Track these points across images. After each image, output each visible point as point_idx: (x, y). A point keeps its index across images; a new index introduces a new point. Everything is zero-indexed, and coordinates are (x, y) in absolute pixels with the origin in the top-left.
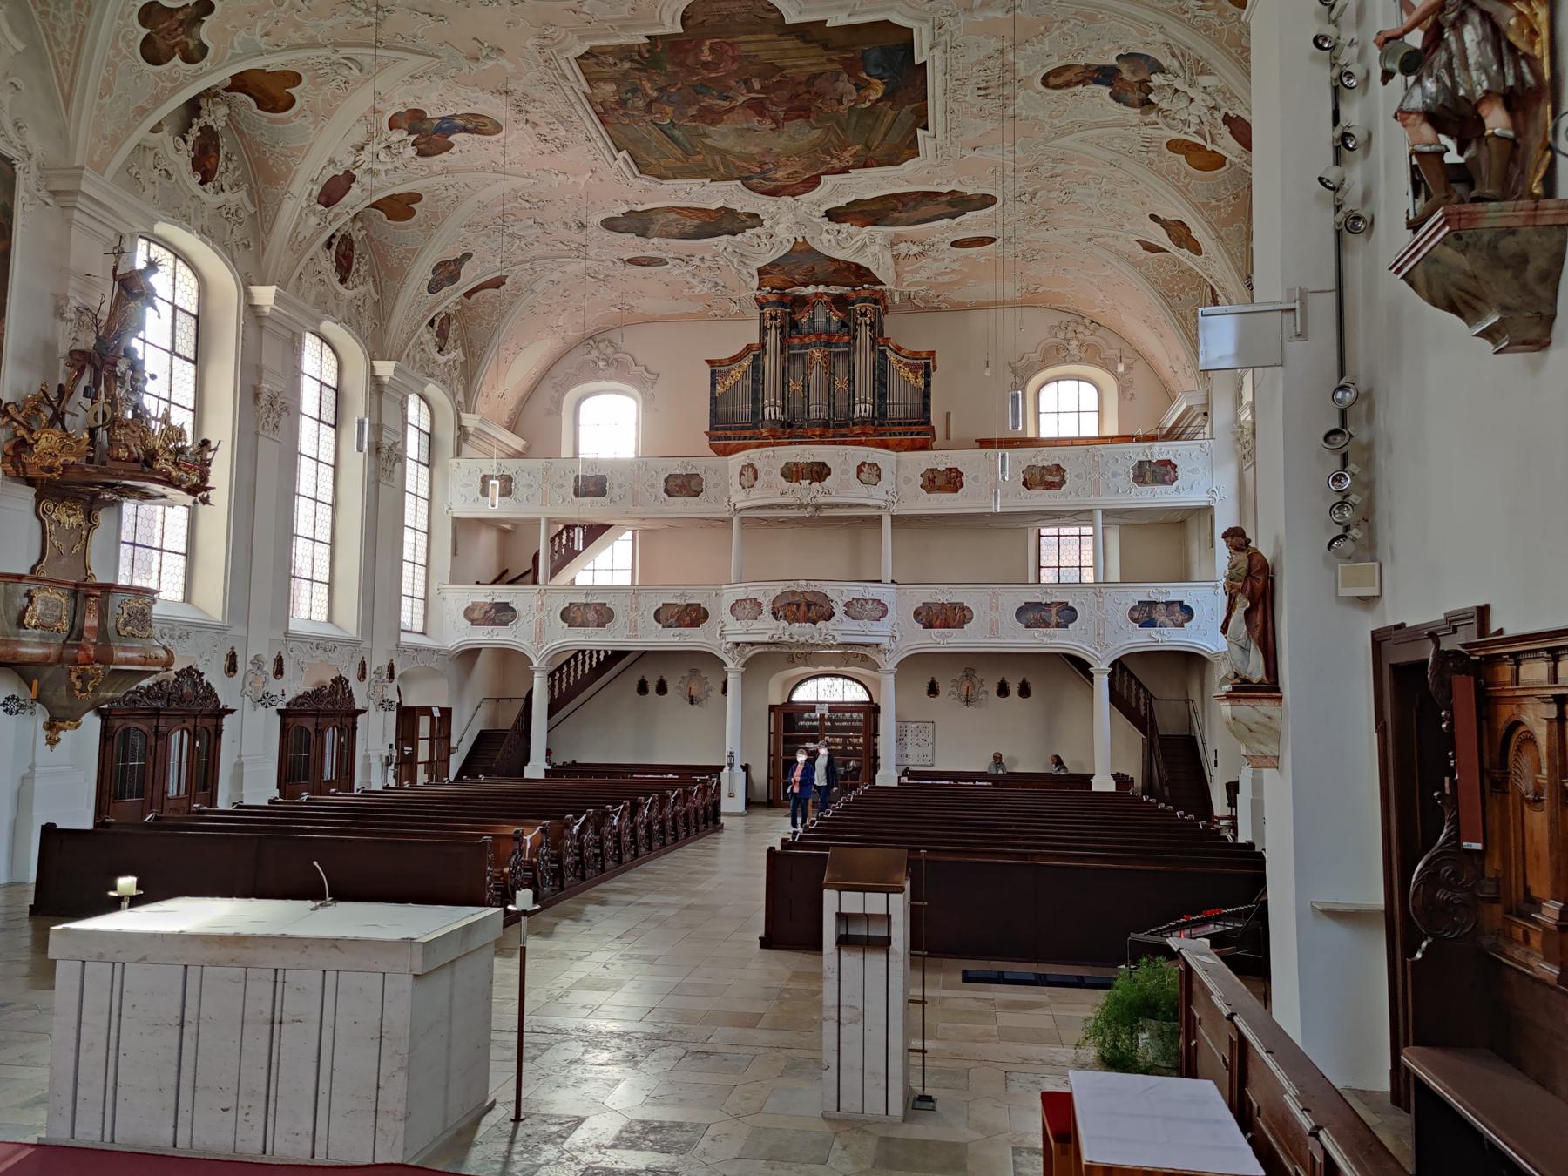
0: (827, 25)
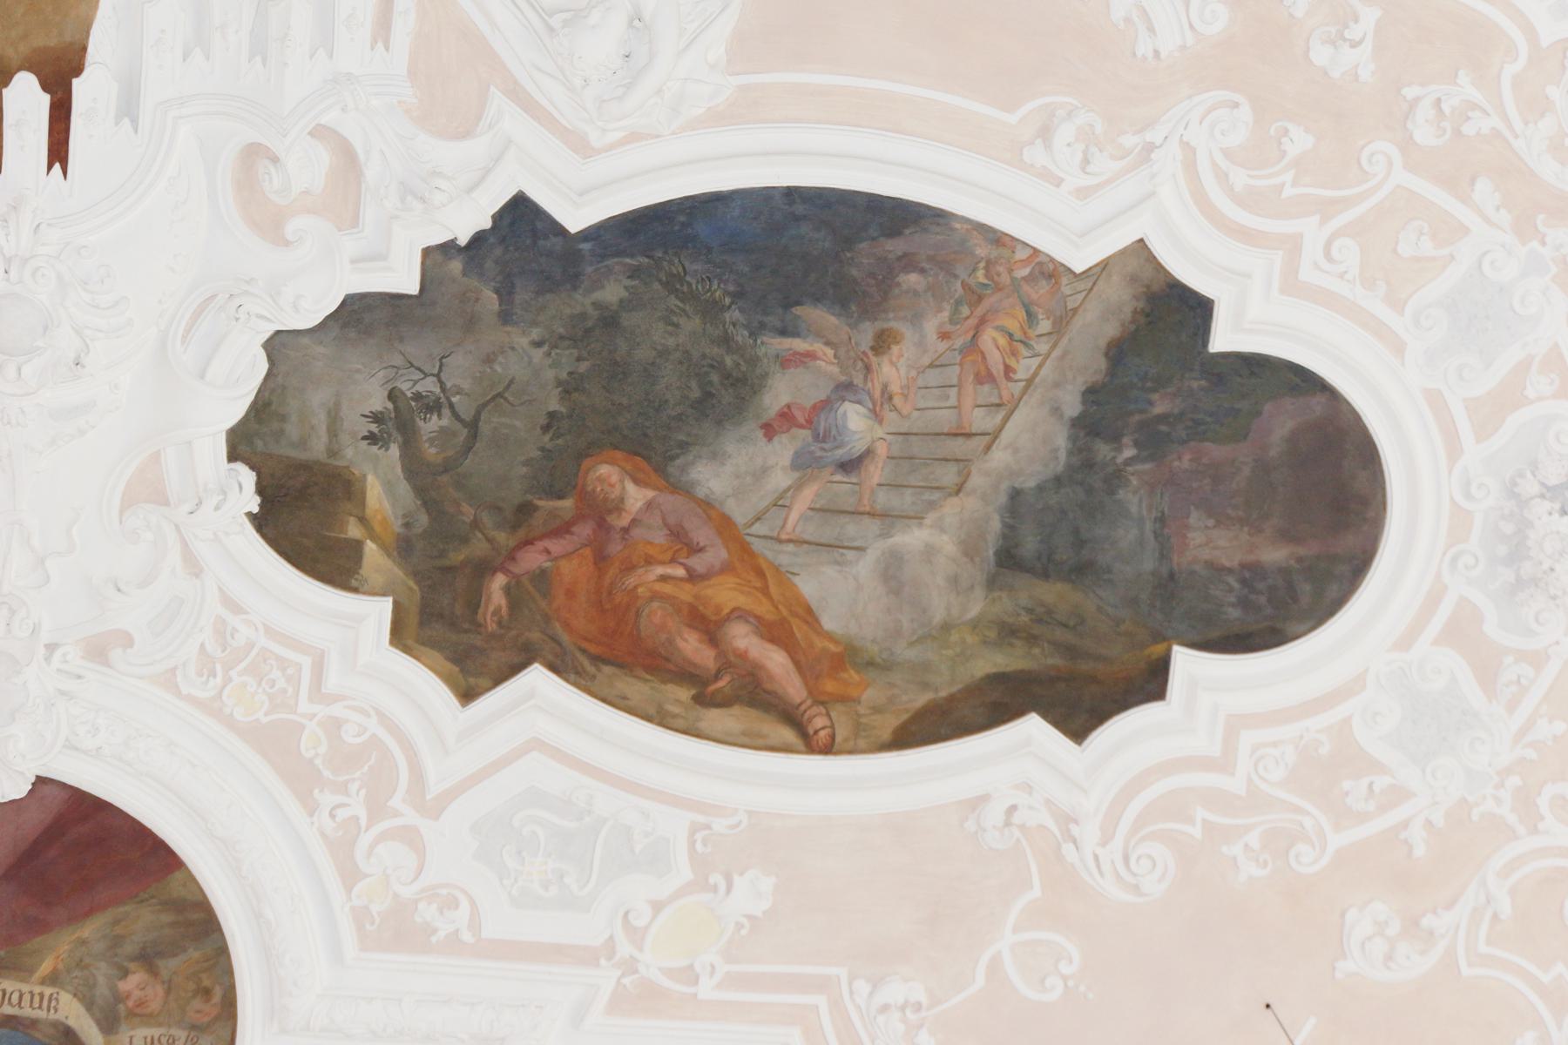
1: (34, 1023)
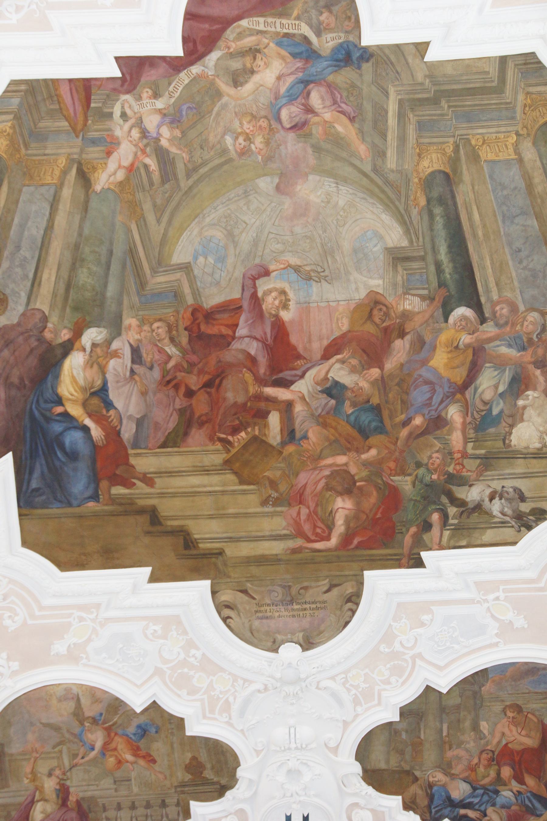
0: (147, 571)
1: (294, 35)
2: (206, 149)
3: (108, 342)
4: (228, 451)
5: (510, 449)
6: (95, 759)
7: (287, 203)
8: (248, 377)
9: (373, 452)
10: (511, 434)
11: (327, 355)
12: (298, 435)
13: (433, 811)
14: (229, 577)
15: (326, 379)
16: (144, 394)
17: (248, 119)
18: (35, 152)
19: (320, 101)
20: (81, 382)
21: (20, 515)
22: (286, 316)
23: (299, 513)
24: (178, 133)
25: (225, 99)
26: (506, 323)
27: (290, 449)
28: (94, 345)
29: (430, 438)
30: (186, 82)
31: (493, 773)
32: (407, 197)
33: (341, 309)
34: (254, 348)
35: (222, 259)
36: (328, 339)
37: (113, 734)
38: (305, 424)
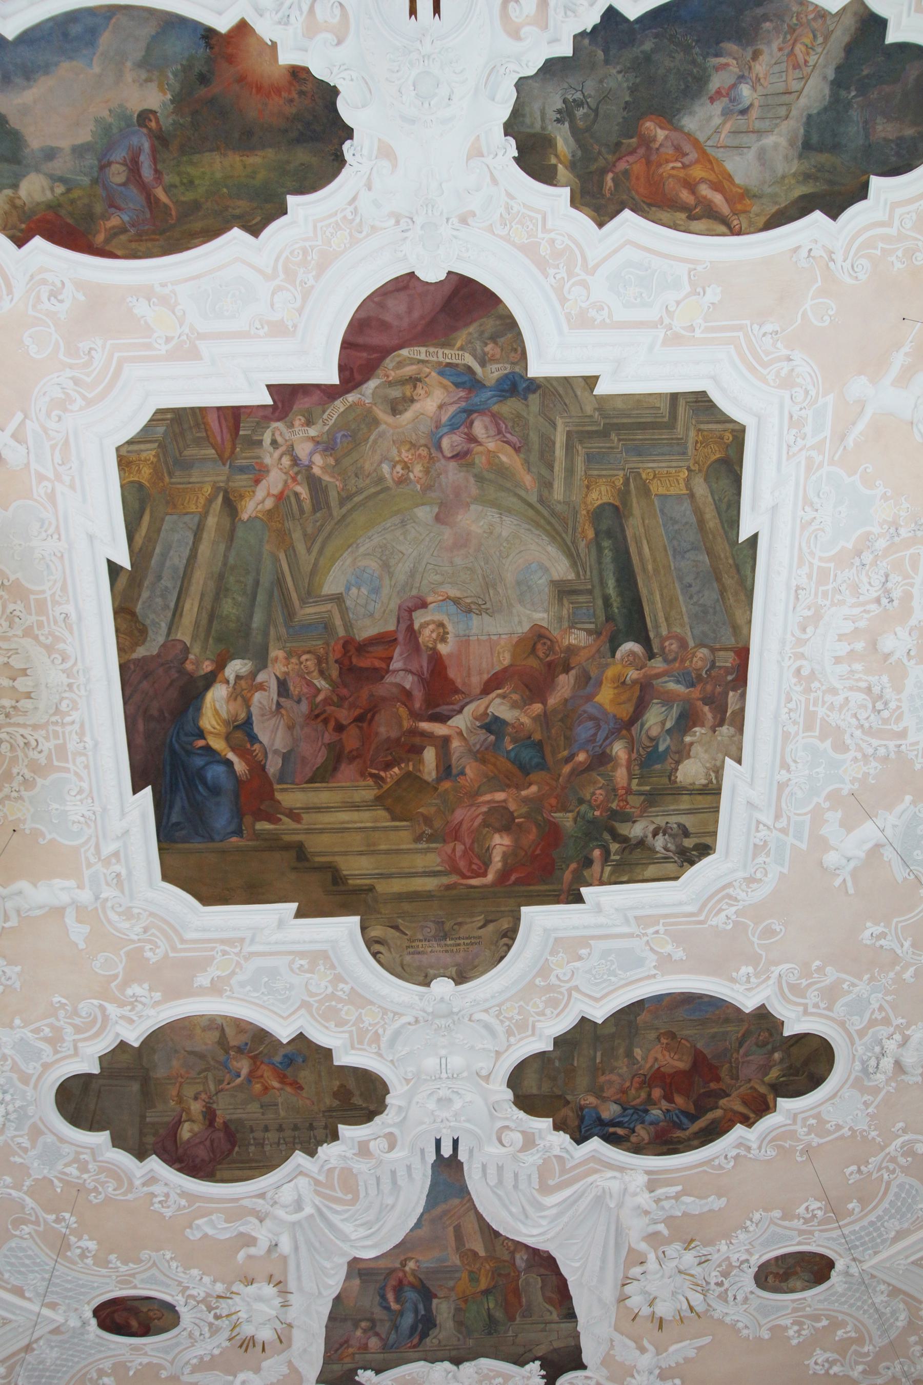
0: (294, 906)
1: (457, 365)
2: (361, 477)
3: (253, 675)
4: (380, 787)
5: (675, 786)
6: (240, 1086)
7: (447, 534)
8: (403, 711)
9: (534, 789)
10: (677, 770)
11: (487, 689)
12: (455, 771)
13: (583, 1130)
14: (381, 913)
15: (485, 714)
16: (290, 728)
17: (407, 447)
18: (179, 480)
19: (483, 431)
20: (224, 715)
21: (160, 849)
22: (443, 649)
23: (454, 850)
24: (331, 461)
25: (383, 427)
26: (675, 659)
27: (446, 785)
28: (238, 678)
29: (594, 774)
30: (342, 410)
31: (643, 1095)
32: (575, 529)
33: (502, 643)
34: (408, 682)
35: (376, 591)
36: (488, 673)
37: (258, 1063)
38: (463, 760)
